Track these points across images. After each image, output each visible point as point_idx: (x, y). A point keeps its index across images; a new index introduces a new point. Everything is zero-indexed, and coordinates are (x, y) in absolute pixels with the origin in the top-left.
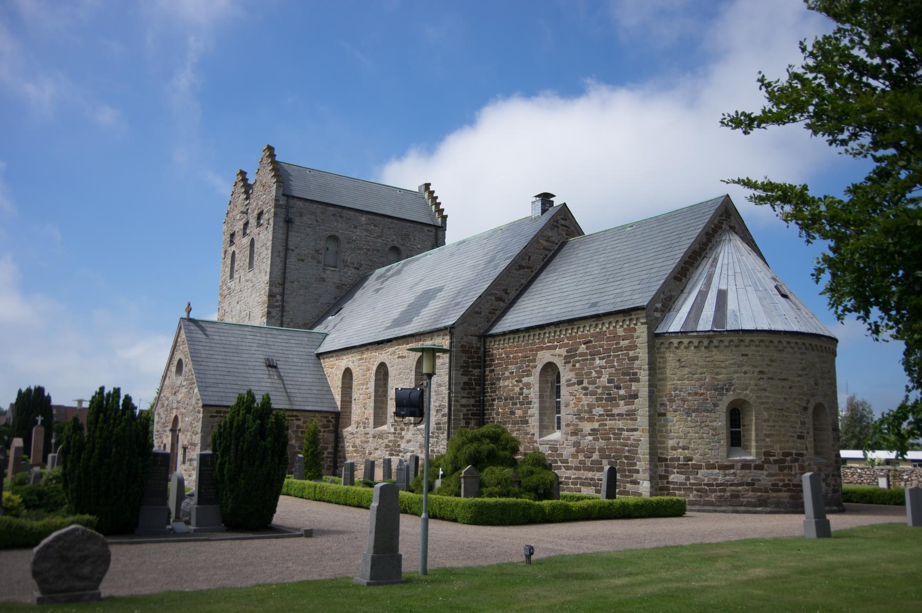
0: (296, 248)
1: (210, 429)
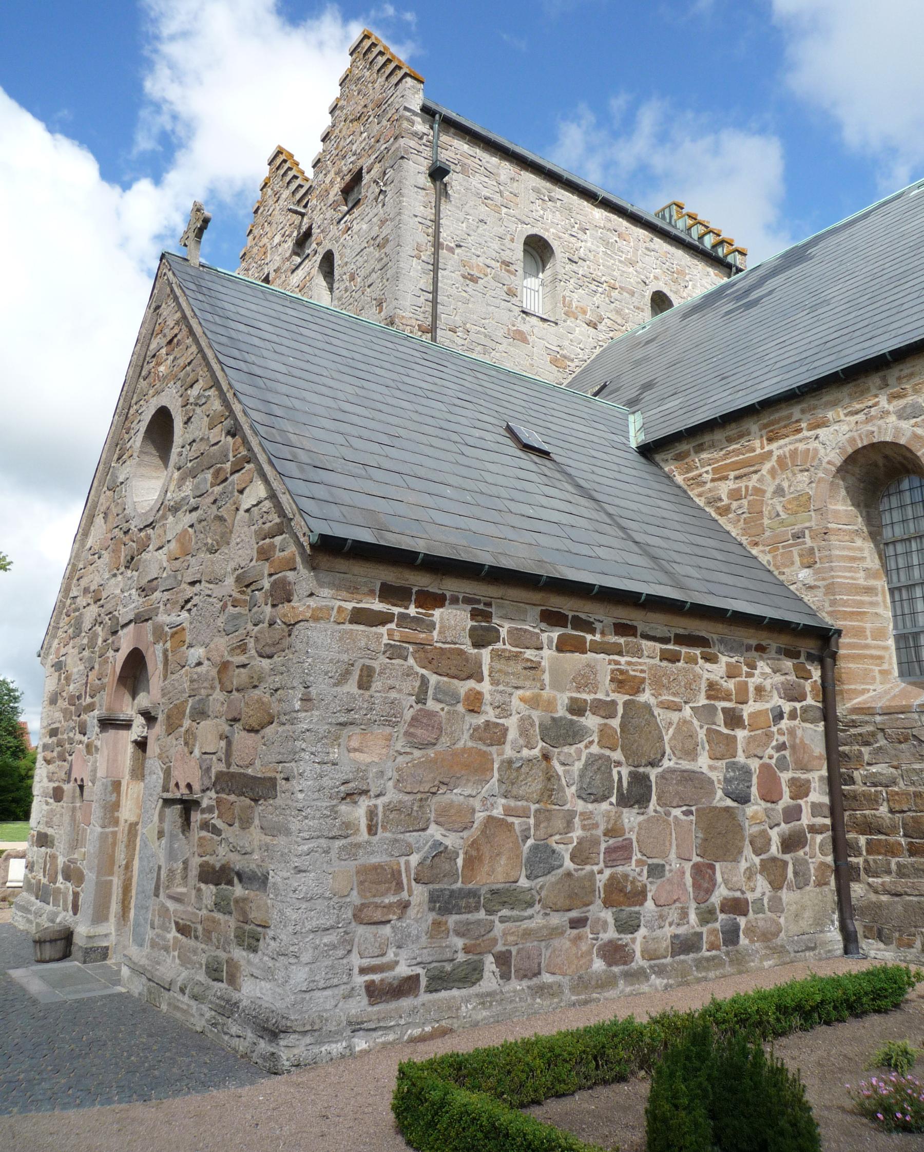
0: (459, 246)
1: (351, 687)
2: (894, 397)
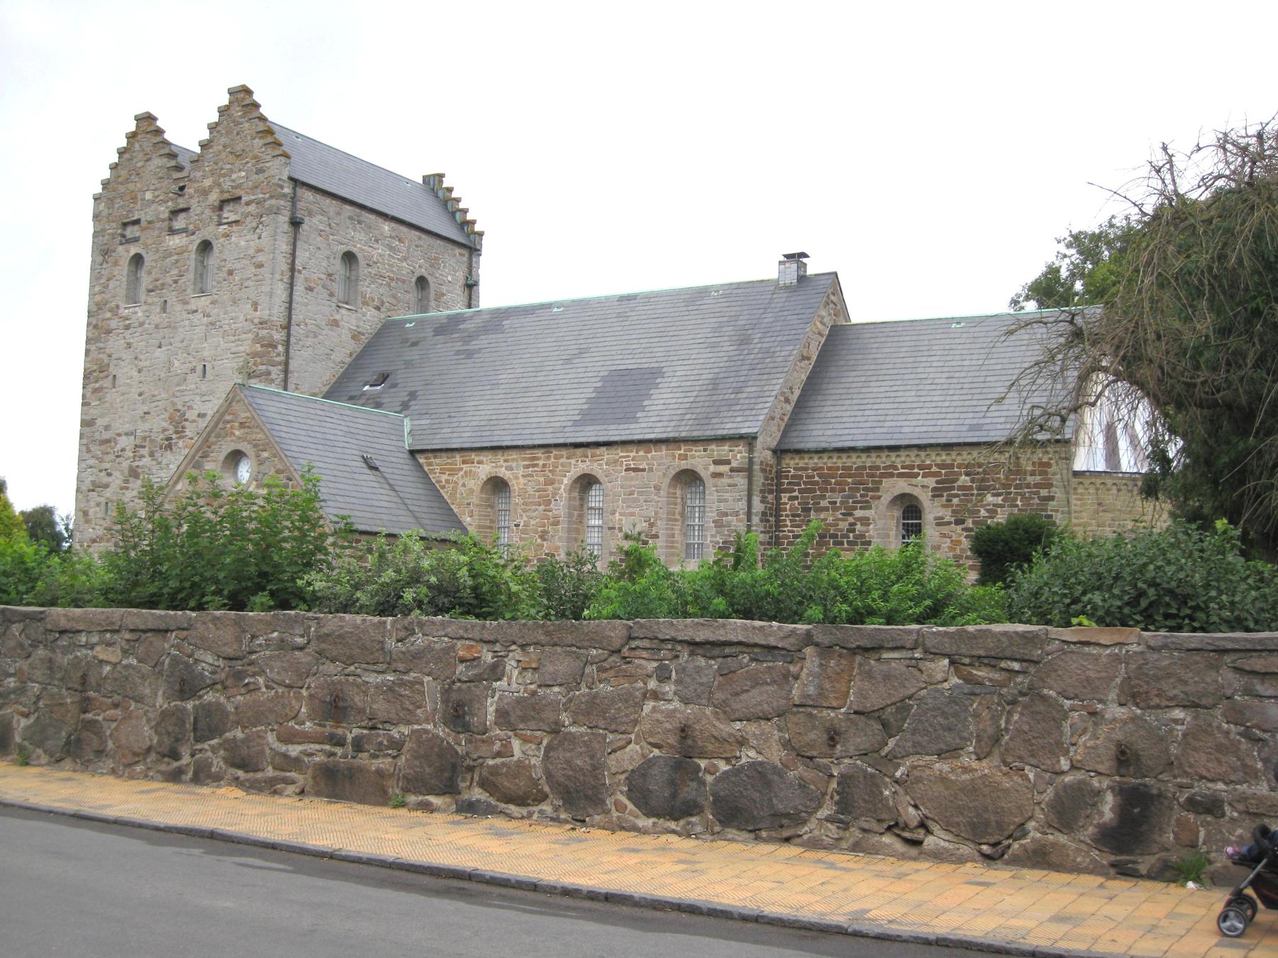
2: (506, 461)
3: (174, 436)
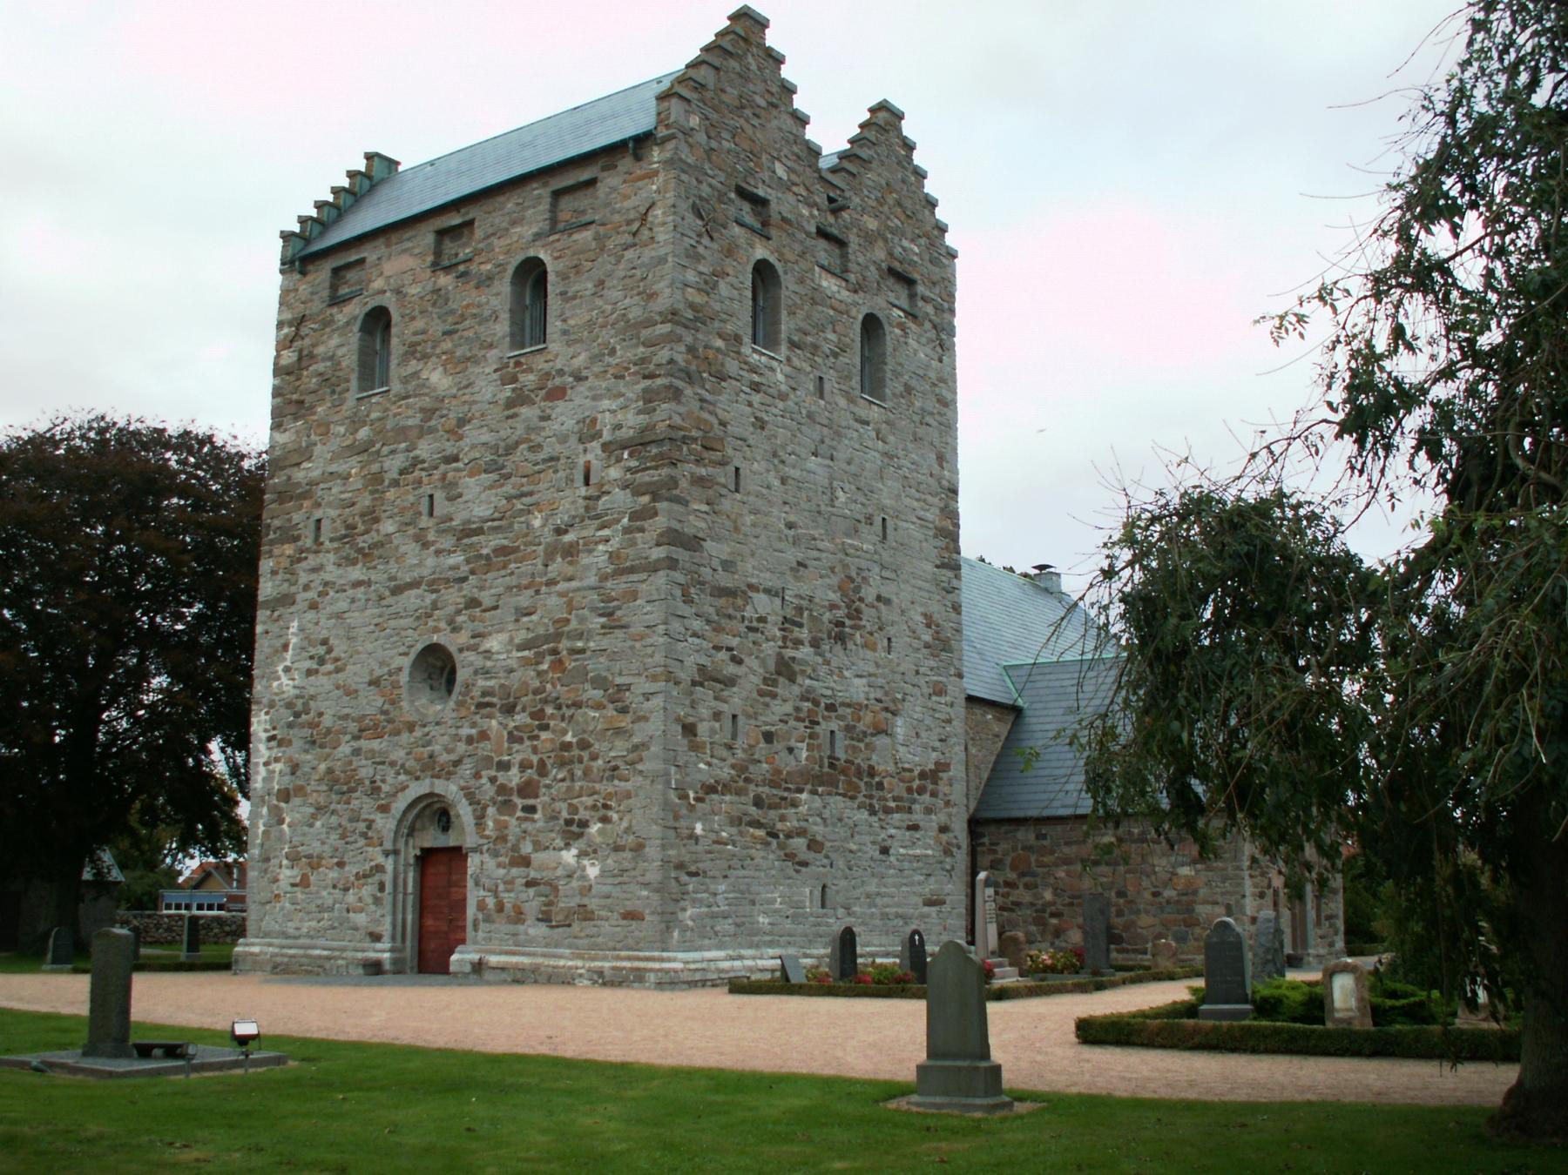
3: (848, 622)
